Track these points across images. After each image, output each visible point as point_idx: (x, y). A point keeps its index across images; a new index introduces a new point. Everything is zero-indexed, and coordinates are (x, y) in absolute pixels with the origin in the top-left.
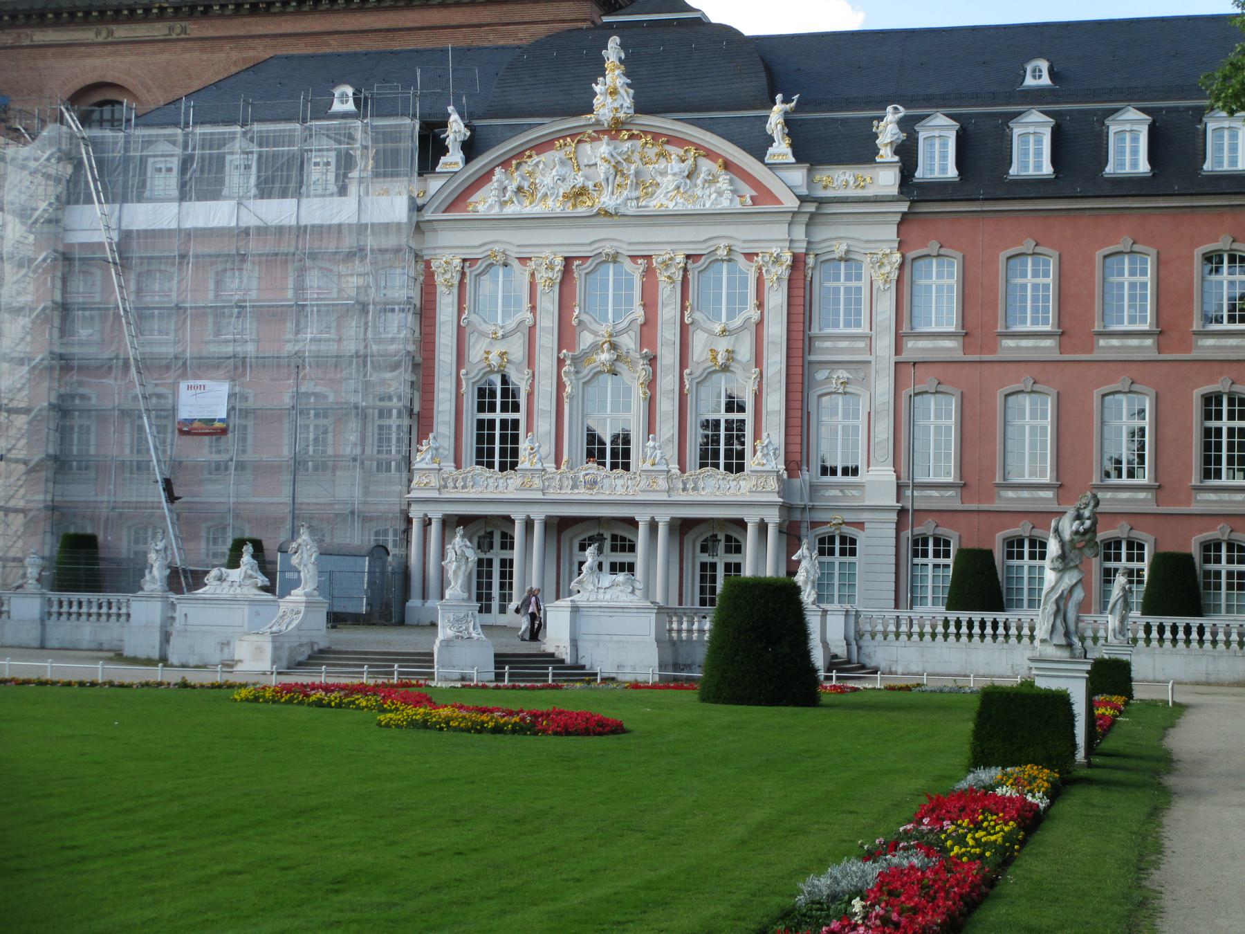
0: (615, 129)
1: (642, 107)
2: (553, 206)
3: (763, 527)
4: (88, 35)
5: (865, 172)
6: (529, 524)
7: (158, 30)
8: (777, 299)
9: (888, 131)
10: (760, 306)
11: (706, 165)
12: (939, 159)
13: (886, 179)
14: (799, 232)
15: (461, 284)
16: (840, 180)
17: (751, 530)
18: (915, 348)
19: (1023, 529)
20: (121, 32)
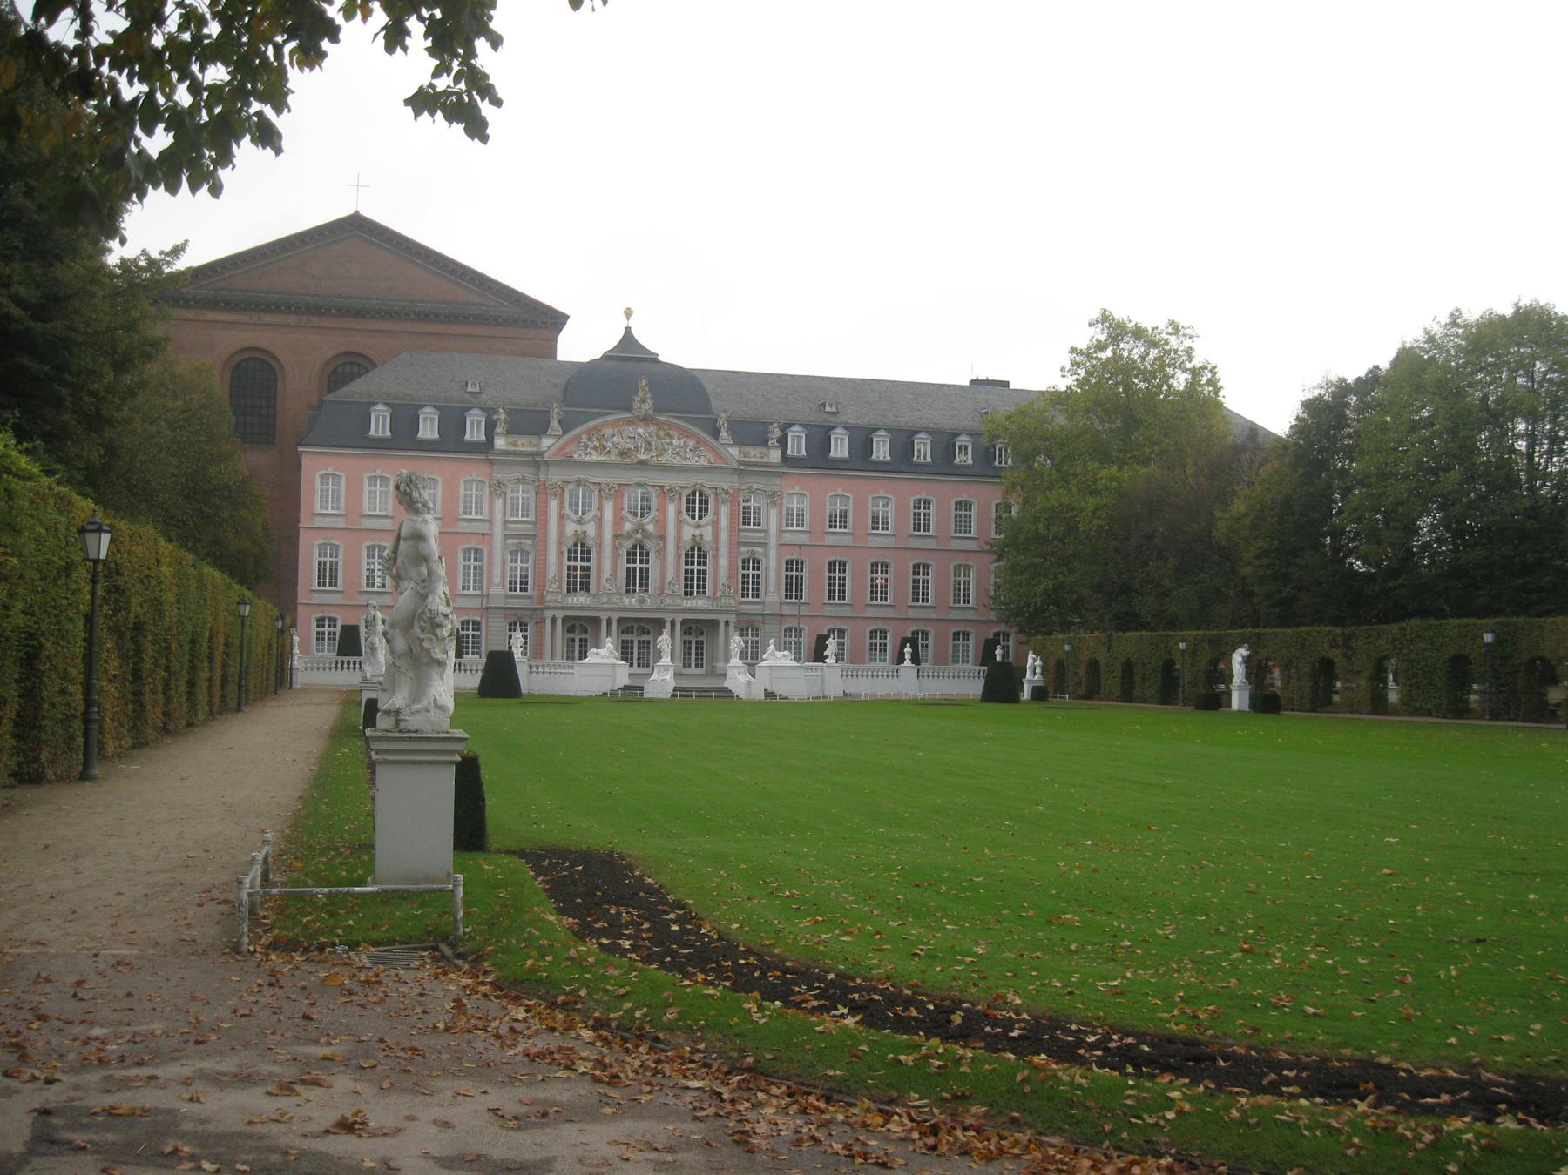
0: (646, 420)
1: (657, 409)
2: (614, 458)
3: (727, 623)
4: (245, 318)
5: (763, 450)
6: (609, 622)
7: (292, 319)
8: (725, 511)
9: (777, 433)
10: (716, 513)
11: (691, 443)
12: (798, 445)
13: (775, 456)
14: (735, 478)
15: (562, 495)
16: (754, 454)
17: (722, 626)
18: (788, 538)
19: (838, 625)
20: (267, 318)
